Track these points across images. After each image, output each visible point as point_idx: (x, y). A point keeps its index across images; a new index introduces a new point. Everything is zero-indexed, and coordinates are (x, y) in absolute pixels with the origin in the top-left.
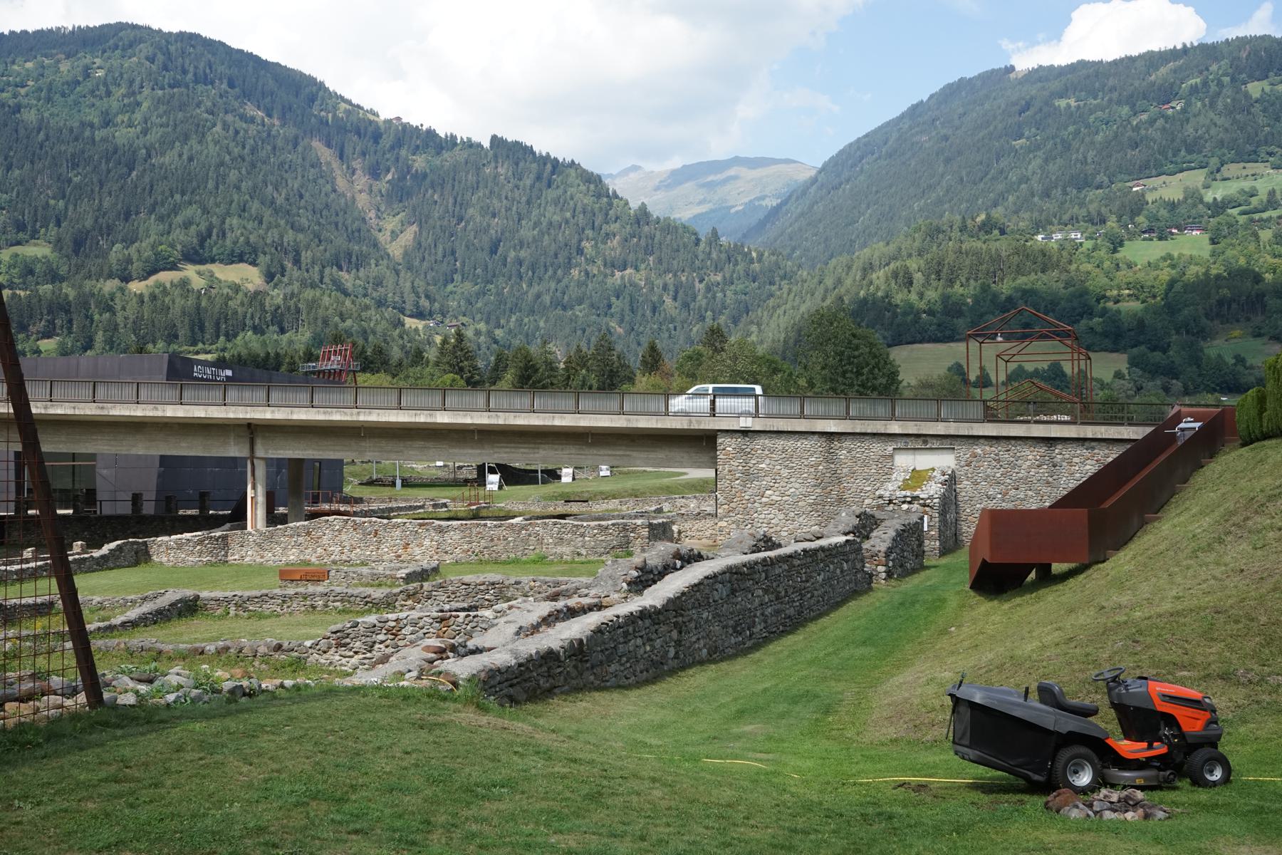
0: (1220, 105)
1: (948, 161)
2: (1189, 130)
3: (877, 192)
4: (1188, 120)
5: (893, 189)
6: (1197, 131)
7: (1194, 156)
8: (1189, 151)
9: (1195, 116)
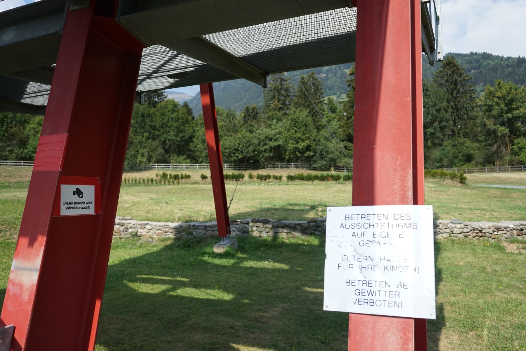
0: (338, 75)
1: (246, 91)
2: (329, 83)
3: (221, 101)
4: (328, 80)
5: (227, 100)
6: (331, 83)
7: (331, 91)
8: (330, 90)
9: (331, 78)
